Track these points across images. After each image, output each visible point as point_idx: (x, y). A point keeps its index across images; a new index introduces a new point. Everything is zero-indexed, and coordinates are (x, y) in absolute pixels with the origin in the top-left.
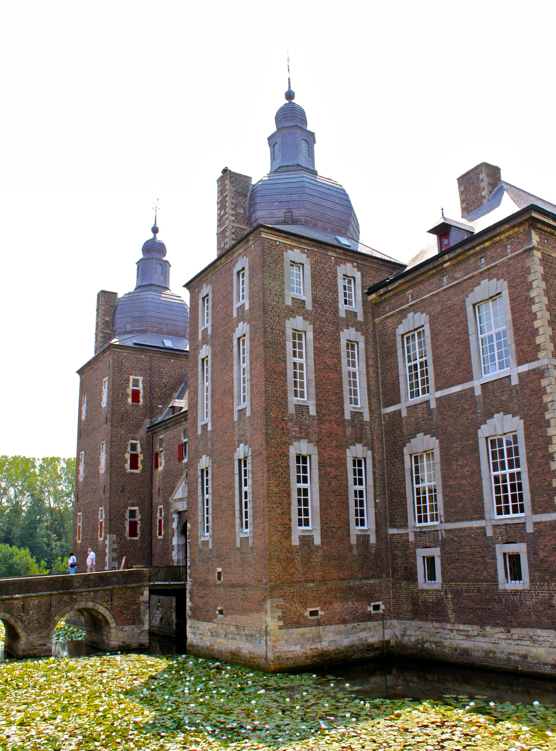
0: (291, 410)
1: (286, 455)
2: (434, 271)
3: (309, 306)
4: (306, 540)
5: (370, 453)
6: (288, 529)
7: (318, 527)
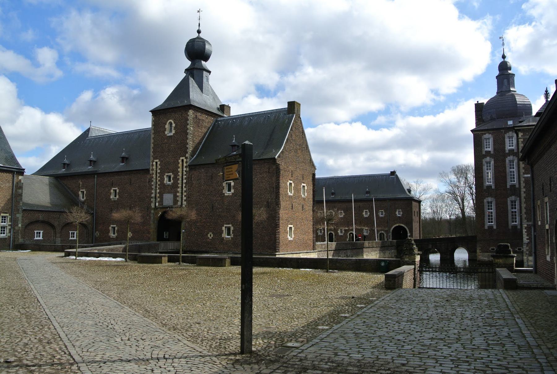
0: (485, 188)
1: (483, 202)
4: (491, 227)
5: (518, 198)
6: (484, 224)
7: (495, 224)
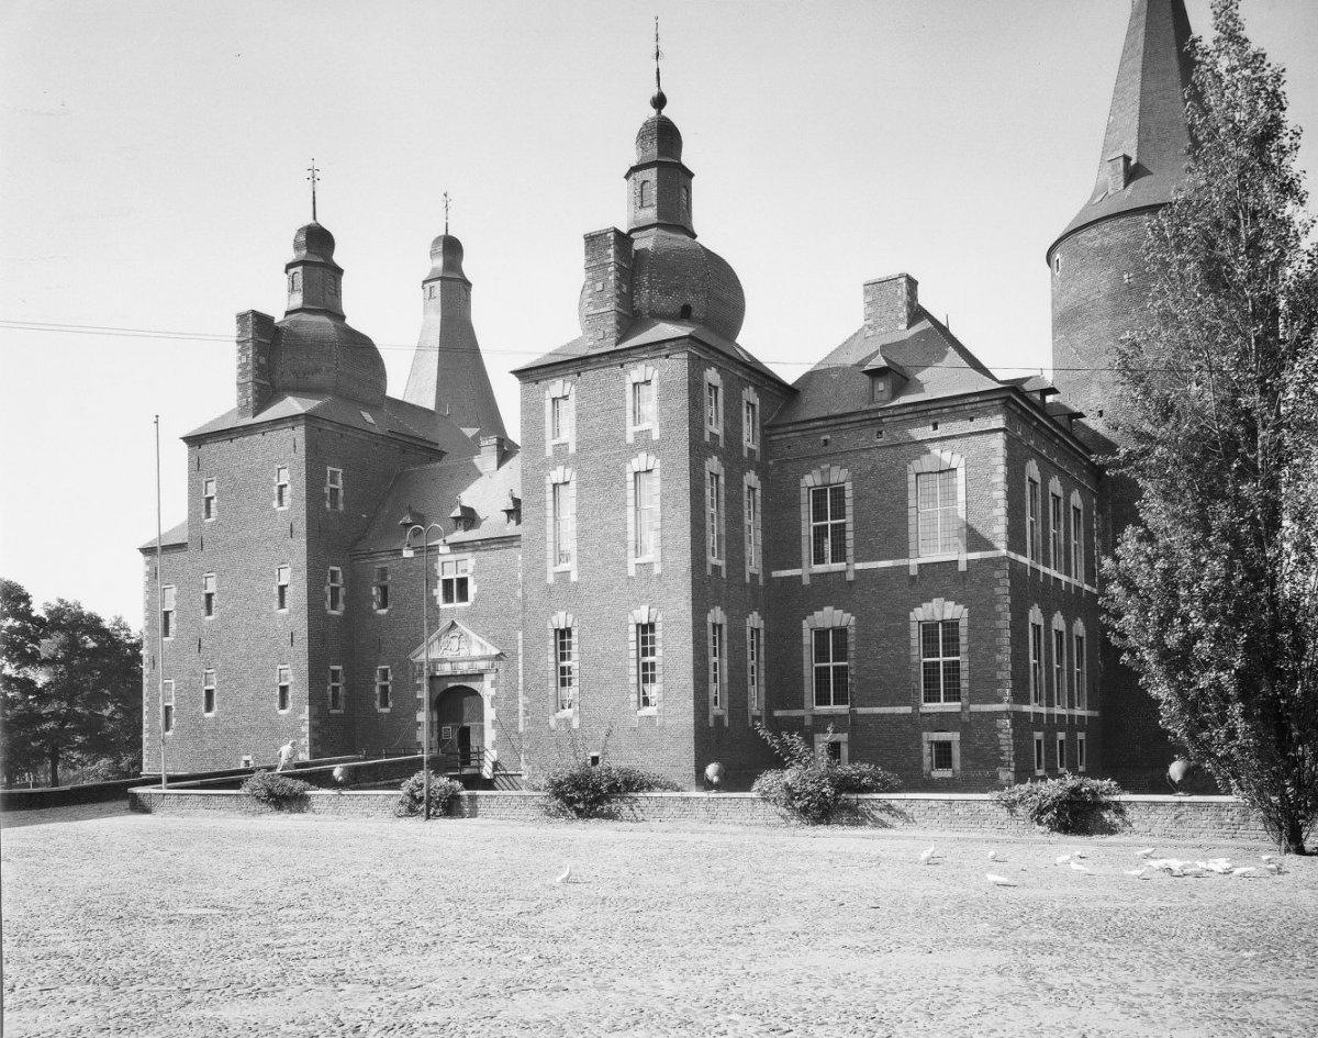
2: (868, 422)
3: (722, 445)
